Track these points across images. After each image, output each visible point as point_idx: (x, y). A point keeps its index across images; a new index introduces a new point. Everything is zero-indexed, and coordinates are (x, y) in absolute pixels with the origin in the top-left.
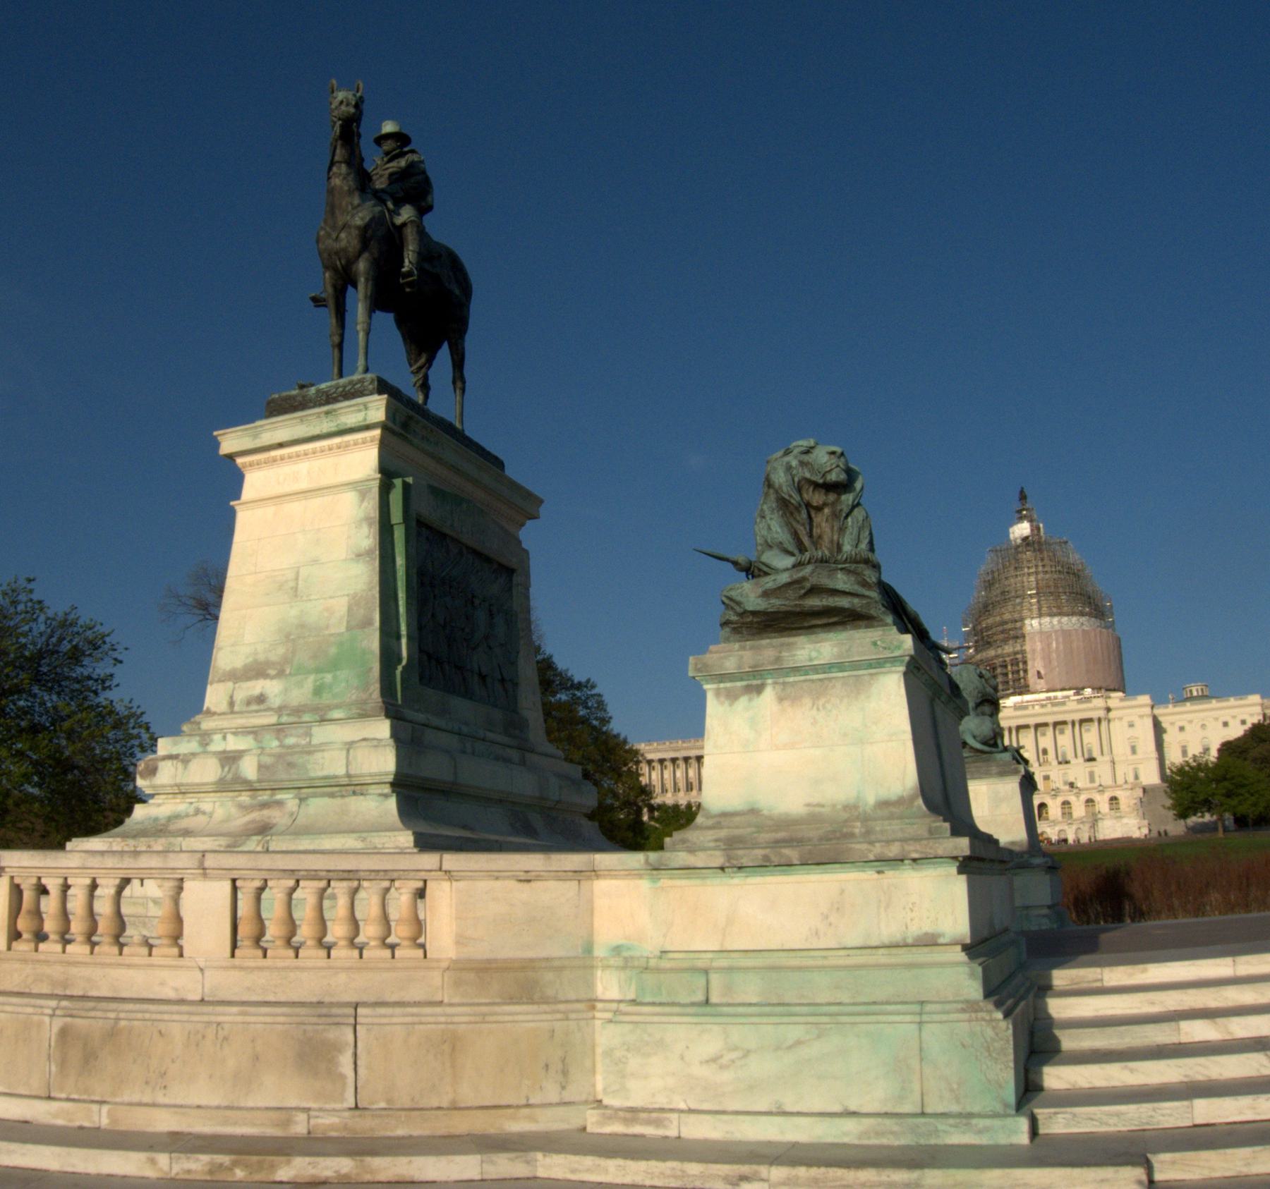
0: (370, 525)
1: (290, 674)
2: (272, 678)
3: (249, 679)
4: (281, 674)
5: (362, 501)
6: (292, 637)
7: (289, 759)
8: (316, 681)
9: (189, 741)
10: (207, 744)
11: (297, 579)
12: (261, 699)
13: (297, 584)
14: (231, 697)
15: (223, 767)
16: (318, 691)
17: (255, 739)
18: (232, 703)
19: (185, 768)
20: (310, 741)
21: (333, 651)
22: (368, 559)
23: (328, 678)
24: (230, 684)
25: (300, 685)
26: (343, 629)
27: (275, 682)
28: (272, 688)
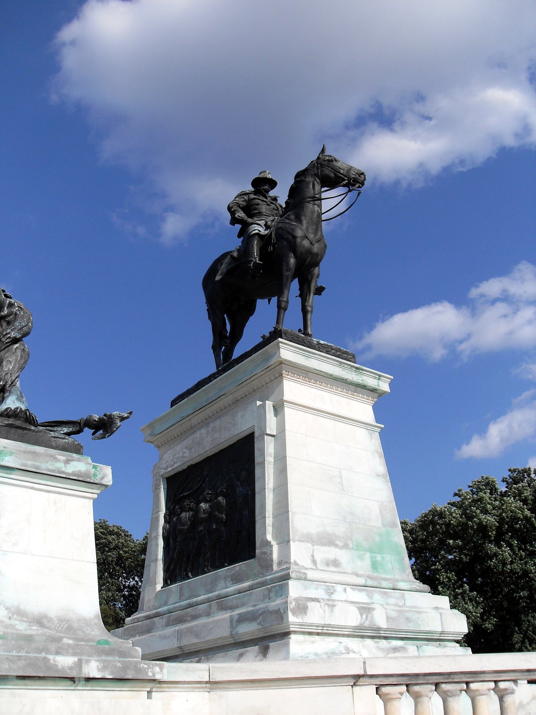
0: (380, 456)
1: (352, 548)
2: (341, 548)
3: (323, 544)
4: (346, 546)
5: (371, 438)
6: (348, 520)
7: (409, 615)
8: (371, 558)
9: (316, 588)
10: (332, 593)
11: (341, 477)
12: (335, 563)
13: (342, 481)
14: (313, 556)
15: (361, 615)
16: (375, 565)
17: (367, 595)
18: (314, 562)
19: (332, 611)
20: (405, 604)
21: (377, 539)
22: (383, 480)
23: (379, 558)
24: (310, 545)
25: (361, 558)
26: (380, 525)
27: (344, 551)
28: (343, 556)
